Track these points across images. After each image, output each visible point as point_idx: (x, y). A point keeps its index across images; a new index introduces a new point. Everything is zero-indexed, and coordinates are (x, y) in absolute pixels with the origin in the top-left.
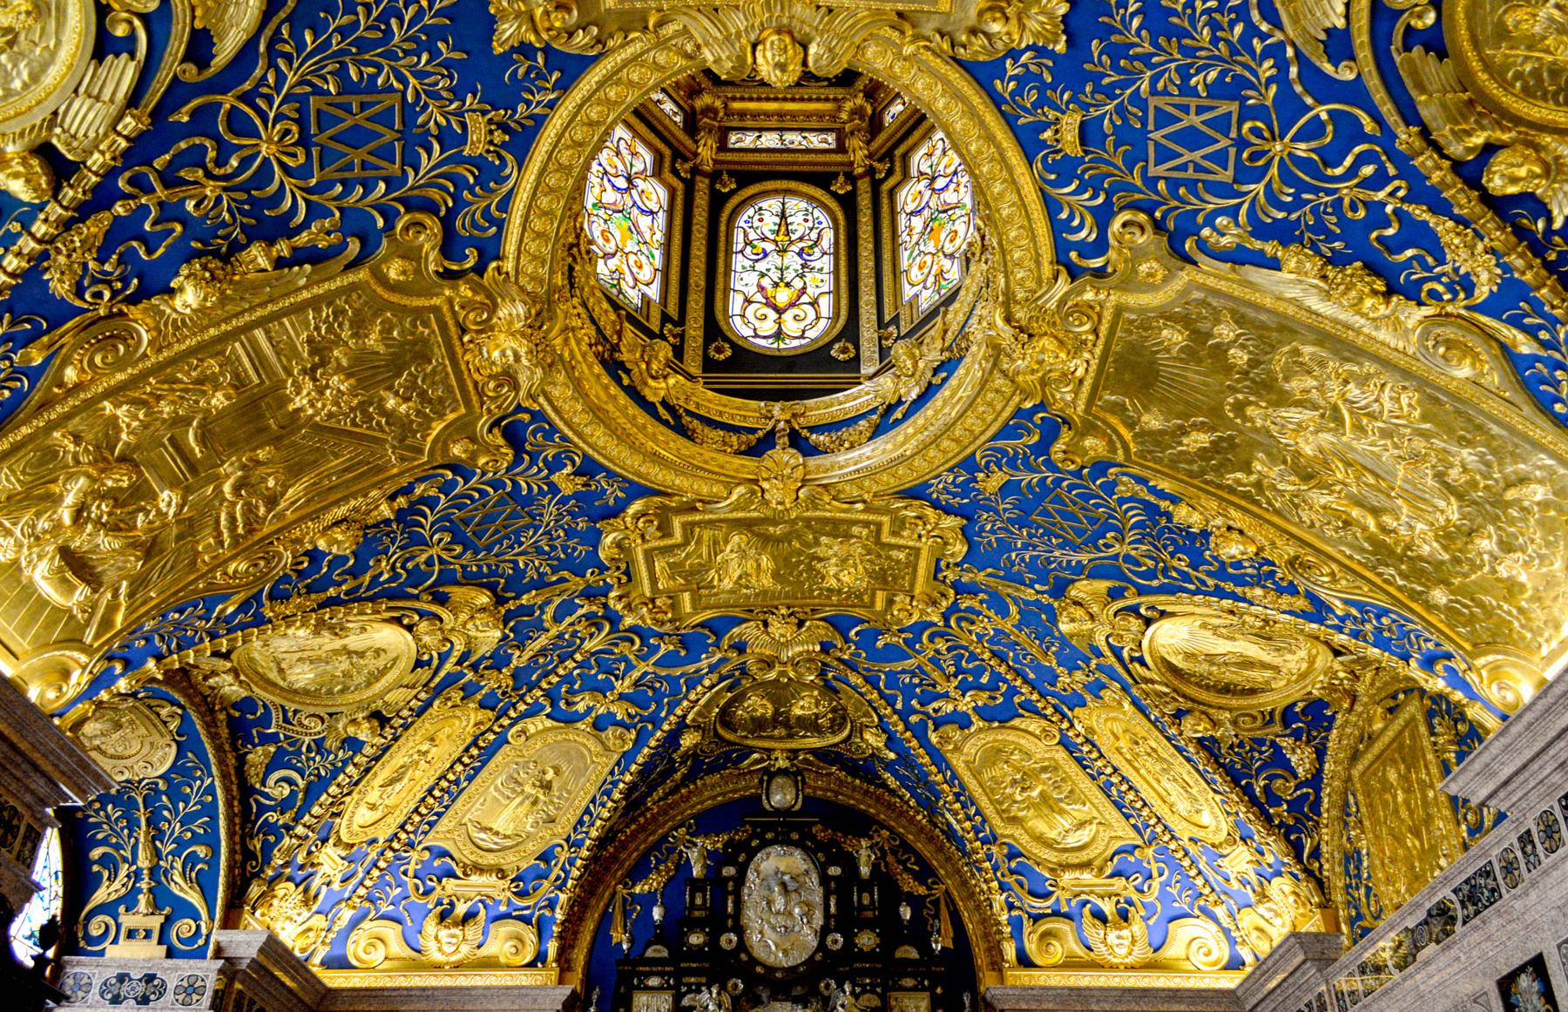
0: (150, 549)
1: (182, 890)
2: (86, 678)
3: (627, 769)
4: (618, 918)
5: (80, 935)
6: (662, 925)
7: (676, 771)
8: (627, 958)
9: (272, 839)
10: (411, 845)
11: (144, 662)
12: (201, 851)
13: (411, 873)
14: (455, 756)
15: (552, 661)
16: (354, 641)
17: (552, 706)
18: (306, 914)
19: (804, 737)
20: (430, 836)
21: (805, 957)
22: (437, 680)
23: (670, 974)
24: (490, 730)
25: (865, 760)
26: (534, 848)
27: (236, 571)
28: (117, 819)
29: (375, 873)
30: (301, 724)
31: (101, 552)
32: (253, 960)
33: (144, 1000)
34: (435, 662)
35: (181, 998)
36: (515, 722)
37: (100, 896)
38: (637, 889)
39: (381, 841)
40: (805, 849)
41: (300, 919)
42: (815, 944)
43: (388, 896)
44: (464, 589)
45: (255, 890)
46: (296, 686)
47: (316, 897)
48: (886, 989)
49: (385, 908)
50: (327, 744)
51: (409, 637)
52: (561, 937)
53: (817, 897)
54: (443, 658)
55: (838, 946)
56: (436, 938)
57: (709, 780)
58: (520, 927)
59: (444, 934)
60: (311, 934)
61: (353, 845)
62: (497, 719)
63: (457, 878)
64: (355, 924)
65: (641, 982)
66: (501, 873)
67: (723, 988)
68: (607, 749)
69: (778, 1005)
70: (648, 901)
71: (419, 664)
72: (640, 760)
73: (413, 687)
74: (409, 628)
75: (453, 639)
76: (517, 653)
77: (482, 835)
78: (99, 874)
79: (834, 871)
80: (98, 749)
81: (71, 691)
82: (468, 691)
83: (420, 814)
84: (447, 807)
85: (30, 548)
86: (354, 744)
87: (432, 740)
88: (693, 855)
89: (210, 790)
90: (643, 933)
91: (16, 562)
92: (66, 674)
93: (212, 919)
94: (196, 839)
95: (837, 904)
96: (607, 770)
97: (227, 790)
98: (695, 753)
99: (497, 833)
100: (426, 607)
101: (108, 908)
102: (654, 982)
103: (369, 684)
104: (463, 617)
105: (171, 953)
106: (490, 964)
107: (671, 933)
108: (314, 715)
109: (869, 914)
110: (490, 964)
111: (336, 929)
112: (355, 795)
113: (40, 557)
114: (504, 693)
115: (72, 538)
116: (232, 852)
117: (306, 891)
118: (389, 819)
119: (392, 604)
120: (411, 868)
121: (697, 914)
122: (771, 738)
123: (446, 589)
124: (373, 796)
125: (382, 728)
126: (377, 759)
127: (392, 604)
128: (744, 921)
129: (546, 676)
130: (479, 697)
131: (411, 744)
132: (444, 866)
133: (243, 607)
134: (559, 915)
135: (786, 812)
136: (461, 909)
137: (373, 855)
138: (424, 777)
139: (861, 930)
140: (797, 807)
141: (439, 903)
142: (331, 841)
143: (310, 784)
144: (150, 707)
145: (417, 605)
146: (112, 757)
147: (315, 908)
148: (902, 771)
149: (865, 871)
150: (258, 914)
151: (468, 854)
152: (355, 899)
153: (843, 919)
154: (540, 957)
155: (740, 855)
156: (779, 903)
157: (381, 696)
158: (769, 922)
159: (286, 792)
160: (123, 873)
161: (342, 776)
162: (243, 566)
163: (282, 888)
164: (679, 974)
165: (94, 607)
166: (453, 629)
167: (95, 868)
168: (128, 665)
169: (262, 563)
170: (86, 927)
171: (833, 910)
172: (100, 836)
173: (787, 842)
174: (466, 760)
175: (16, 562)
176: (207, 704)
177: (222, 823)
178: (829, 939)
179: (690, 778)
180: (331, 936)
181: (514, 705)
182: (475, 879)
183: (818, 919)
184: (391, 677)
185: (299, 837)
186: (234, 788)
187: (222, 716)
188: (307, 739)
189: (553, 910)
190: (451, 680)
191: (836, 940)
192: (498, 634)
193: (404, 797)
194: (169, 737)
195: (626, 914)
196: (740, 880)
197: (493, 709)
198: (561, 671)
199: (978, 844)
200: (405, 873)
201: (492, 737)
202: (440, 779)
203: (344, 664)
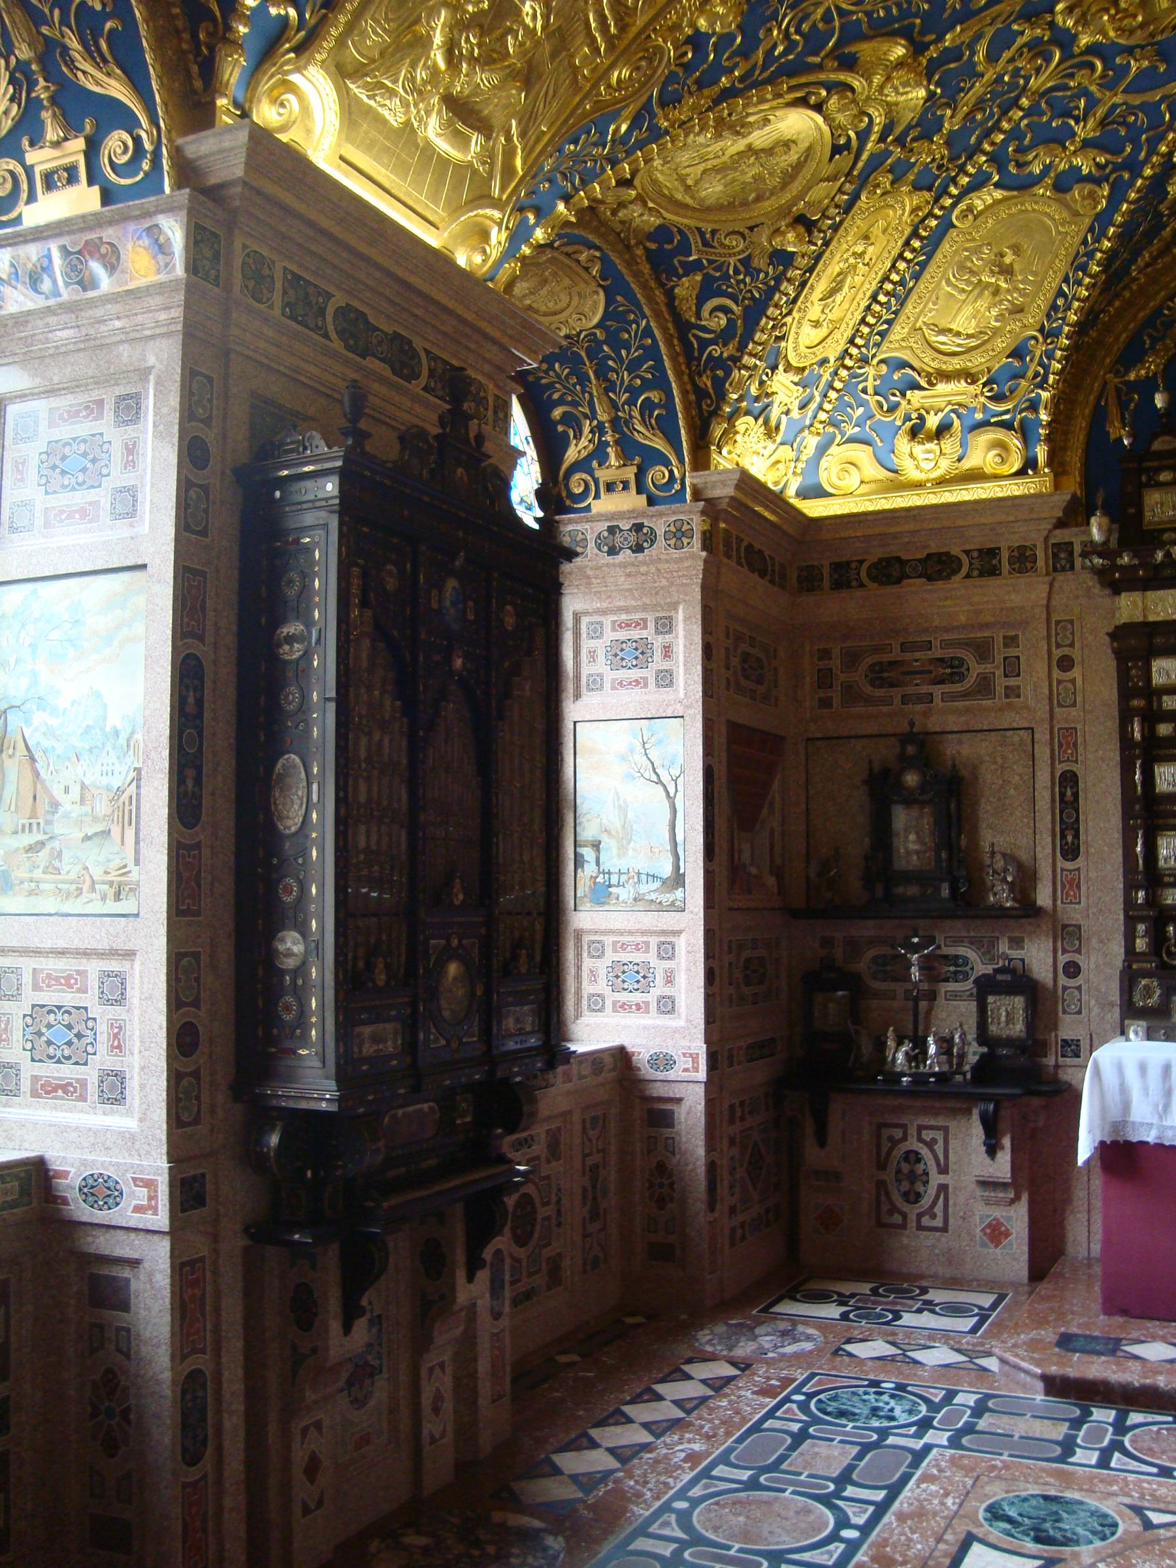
0: (528, 77)
1: (646, 438)
2: (504, 235)
3: (1103, 234)
4: (1114, 410)
5: (564, 494)
9: (720, 373)
10: (864, 361)
11: (555, 206)
12: (655, 396)
13: (870, 390)
14: (895, 253)
15: (992, 114)
16: (759, 138)
17: (999, 173)
18: (771, 446)
20: (884, 347)
22: (860, 165)
24: (931, 214)
26: (1002, 344)
27: (619, 80)
28: (567, 377)
29: (833, 395)
30: (722, 245)
31: (483, 92)
32: (732, 498)
33: (638, 549)
34: (854, 143)
35: (672, 542)
36: (958, 199)
37: (572, 454)
38: (1132, 376)
39: (832, 360)
41: (767, 453)
43: (850, 417)
44: (874, 44)
45: (717, 431)
46: (710, 201)
47: (777, 428)
49: (852, 431)
50: (755, 263)
51: (819, 119)
52: (1049, 439)
54: (863, 136)
56: (911, 455)
58: (1000, 434)
59: (918, 449)
60: (780, 466)
61: (804, 369)
62: (936, 200)
63: (922, 388)
64: (822, 450)
65: (1150, 479)
66: (970, 377)
68: (1076, 214)
70: (1147, 387)
71: (836, 150)
72: (1119, 219)
73: (834, 178)
74: (818, 108)
75: (871, 111)
76: (949, 112)
77: (942, 338)
78: (565, 433)
80: (530, 308)
81: (494, 253)
82: (898, 173)
83: (868, 325)
84: (896, 313)
85: (416, 105)
86: (783, 259)
87: (866, 238)
89: (648, 332)
90: (1147, 424)
91: (408, 123)
92: (485, 235)
93: (681, 460)
94: (647, 386)
96: (1078, 240)
97: (664, 330)
99: (958, 334)
100: (833, 76)
101: (581, 465)
102: (1165, 476)
103: (784, 185)
104: (877, 80)
105: (651, 501)
106: (975, 476)
108: (734, 233)
110: (975, 476)
111: (804, 458)
112: (795, 313)
113: (428, 113)
114: (939, 167)
115: (452, 83)
116: (684, 393)
117: (766, 423)
118: (837, 335)
119: (793, 82)
120: (870, 385)
123: (853, 49)
124: (814, 312)
125: (810, 233)
126: (811, 270)
127: (793, 82)
129: (987, 134)
130: (911, 177)
131: (845, 246)
132: (905, 378)
133: (635, 123)
134: (1044, 417)
136: (932, 422)
137: (826, 377)
138: (864, 283)
141: (908, 418)
142: (781, 367)
143: (746, 309)
144: (568, 255)
145: (822, 77)
146: (545, 315)
147: (779, 439)
150: (724, 451)
151: (931, 362)
152: (817, 425)
154: (1030, 464)
157: (801, 196)
159: (723, 322)
160: (586, 429)
161: (777, 297)
162: (625, 73)
163: (743, 423)
165: (492, 157)
166: (868, 98)
167: (560, 428)
168: (539, 212)
169: (643, 63)
170: (567, 486)
172: (556, 396)
174: (908, 255)
175: (408, 123)
176: (623, 238)
177: (667, 364)
180: (801, 465)
181: (954, 181)
182: (942, 387)
184: (807, 173)
185: (747, 368)
186: (670, 325)
187: (639, 252)
188: (732, 261)
190: (876, 162)
192: (922, 93)
193: (848, 308)
194: (594, 284)
195: (1123, 406)
197: (929, 189)
198: (1005, 125)
200: (864, 391)
201: (934, 223)
202: (882, 282)
203: (751, 171)
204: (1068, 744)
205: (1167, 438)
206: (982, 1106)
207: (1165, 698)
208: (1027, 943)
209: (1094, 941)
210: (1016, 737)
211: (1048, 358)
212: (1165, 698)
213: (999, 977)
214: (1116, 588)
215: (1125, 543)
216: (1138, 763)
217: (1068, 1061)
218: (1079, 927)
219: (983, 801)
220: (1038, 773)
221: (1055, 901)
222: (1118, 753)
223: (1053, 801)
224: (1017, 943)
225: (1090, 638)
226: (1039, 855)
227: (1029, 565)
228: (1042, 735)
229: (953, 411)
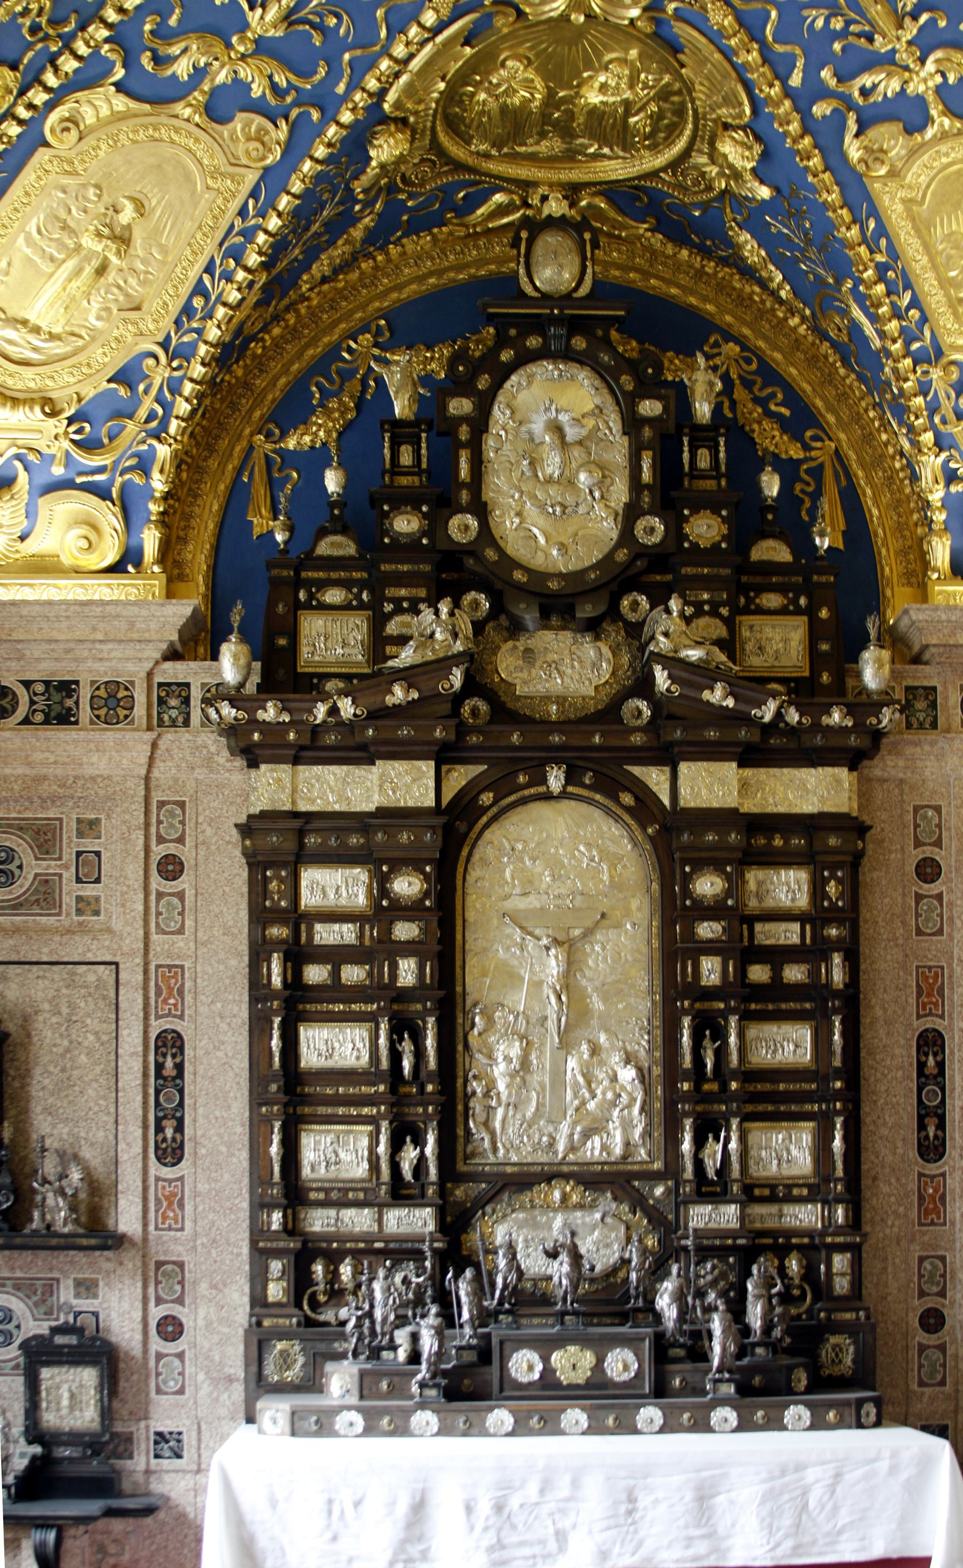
6: (342, 502)
7: (354, 220)
8: (282, 556)
19: (597, 157)
21: (597, 555)
23: (362, 585)
25: (705, 206)
40: (599, 370)
42: (615, 535)
48: (737, 611)
53: (617, 451)
55: (656, 539)
57: (410, 244)
65: (311, 596)
67: (456, 604)
69: (549, 635)
79: (650, 408)
88: (393, 378)
95: (653, 466)
98: (392, 189)
102: (334, 596)
107: (360, 514)
109: (710, 484)
121: (404, 481)
122: (533, 158)
128: (488, 494)
134: (159, 484)
135: (567, 298)
139: (695, 510)
140: (584, 291)
148: (777, 227)
149: (703, 410)
153: (667, 492)
155: (482, 378)
156: (552, 464)
158: (533, 497)
164: (377, 584)
171: (646, 475)
173: (567, 355)
178: (641, 525)
179: (378, 238)
183: (620, 493)
189: (147, 474)
191: (652, 531)
196: (480, 423)
199: (908, 362)
204: (170, 989)
205: (338, 538)
206: (38, 1535)
207: (318, 927)
208: (102, 1289)
209: (203, 1287)
210: (91, 975)
211: (172, 394)
212: (318, 927)
213: (59, 1340)
214: (253, 757)
215: (270, 686)
216: (277, 1020)
217: (165, 1463)
218: (181, 1265)
219: (37, 1071)
220: (124, 1033)
221: (145, 1225)
222: (245, 1006)
223: (145, 1075)
224: (86, 1287)
225: (209, 831)
226: (123, 1157)
227: (122, 713)
228: (131, 975)
229: (18, 457)
